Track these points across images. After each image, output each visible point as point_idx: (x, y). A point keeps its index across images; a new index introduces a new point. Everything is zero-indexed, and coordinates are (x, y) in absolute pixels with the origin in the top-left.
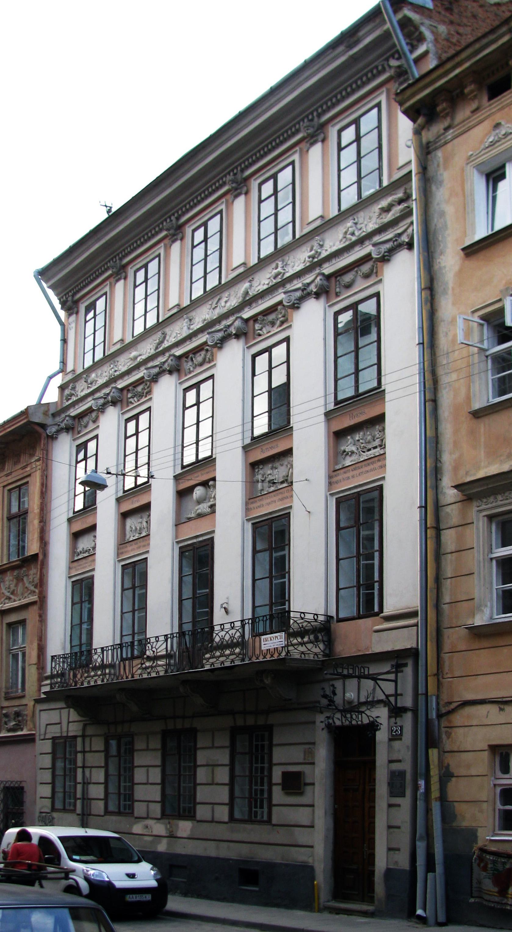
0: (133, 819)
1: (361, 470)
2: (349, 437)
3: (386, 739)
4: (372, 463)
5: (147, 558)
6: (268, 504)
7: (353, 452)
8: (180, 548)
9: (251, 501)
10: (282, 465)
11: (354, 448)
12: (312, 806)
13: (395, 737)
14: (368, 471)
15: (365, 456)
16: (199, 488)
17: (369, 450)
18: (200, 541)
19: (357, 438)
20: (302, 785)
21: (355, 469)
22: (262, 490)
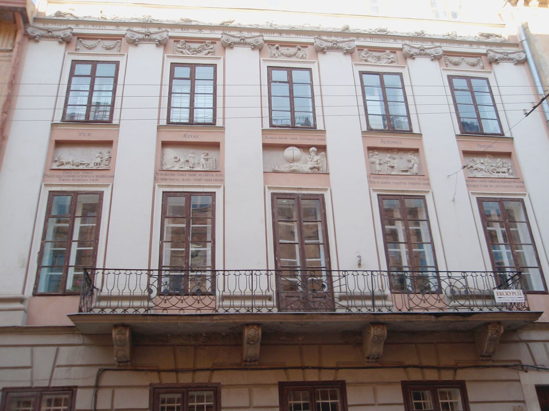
1: (498, 184)
5: (215, 193)
6: (398, 183)
7: (481, 170)
8: (273, 194)
9: (373, 176)
11: (483, 167)
14: (505, 186)
15: (496, 175)
16: (295, 148)
17: (499, 172)
18: (304, 194)
19: (482, 162)
21: (492, 181)
22: (380, 171)
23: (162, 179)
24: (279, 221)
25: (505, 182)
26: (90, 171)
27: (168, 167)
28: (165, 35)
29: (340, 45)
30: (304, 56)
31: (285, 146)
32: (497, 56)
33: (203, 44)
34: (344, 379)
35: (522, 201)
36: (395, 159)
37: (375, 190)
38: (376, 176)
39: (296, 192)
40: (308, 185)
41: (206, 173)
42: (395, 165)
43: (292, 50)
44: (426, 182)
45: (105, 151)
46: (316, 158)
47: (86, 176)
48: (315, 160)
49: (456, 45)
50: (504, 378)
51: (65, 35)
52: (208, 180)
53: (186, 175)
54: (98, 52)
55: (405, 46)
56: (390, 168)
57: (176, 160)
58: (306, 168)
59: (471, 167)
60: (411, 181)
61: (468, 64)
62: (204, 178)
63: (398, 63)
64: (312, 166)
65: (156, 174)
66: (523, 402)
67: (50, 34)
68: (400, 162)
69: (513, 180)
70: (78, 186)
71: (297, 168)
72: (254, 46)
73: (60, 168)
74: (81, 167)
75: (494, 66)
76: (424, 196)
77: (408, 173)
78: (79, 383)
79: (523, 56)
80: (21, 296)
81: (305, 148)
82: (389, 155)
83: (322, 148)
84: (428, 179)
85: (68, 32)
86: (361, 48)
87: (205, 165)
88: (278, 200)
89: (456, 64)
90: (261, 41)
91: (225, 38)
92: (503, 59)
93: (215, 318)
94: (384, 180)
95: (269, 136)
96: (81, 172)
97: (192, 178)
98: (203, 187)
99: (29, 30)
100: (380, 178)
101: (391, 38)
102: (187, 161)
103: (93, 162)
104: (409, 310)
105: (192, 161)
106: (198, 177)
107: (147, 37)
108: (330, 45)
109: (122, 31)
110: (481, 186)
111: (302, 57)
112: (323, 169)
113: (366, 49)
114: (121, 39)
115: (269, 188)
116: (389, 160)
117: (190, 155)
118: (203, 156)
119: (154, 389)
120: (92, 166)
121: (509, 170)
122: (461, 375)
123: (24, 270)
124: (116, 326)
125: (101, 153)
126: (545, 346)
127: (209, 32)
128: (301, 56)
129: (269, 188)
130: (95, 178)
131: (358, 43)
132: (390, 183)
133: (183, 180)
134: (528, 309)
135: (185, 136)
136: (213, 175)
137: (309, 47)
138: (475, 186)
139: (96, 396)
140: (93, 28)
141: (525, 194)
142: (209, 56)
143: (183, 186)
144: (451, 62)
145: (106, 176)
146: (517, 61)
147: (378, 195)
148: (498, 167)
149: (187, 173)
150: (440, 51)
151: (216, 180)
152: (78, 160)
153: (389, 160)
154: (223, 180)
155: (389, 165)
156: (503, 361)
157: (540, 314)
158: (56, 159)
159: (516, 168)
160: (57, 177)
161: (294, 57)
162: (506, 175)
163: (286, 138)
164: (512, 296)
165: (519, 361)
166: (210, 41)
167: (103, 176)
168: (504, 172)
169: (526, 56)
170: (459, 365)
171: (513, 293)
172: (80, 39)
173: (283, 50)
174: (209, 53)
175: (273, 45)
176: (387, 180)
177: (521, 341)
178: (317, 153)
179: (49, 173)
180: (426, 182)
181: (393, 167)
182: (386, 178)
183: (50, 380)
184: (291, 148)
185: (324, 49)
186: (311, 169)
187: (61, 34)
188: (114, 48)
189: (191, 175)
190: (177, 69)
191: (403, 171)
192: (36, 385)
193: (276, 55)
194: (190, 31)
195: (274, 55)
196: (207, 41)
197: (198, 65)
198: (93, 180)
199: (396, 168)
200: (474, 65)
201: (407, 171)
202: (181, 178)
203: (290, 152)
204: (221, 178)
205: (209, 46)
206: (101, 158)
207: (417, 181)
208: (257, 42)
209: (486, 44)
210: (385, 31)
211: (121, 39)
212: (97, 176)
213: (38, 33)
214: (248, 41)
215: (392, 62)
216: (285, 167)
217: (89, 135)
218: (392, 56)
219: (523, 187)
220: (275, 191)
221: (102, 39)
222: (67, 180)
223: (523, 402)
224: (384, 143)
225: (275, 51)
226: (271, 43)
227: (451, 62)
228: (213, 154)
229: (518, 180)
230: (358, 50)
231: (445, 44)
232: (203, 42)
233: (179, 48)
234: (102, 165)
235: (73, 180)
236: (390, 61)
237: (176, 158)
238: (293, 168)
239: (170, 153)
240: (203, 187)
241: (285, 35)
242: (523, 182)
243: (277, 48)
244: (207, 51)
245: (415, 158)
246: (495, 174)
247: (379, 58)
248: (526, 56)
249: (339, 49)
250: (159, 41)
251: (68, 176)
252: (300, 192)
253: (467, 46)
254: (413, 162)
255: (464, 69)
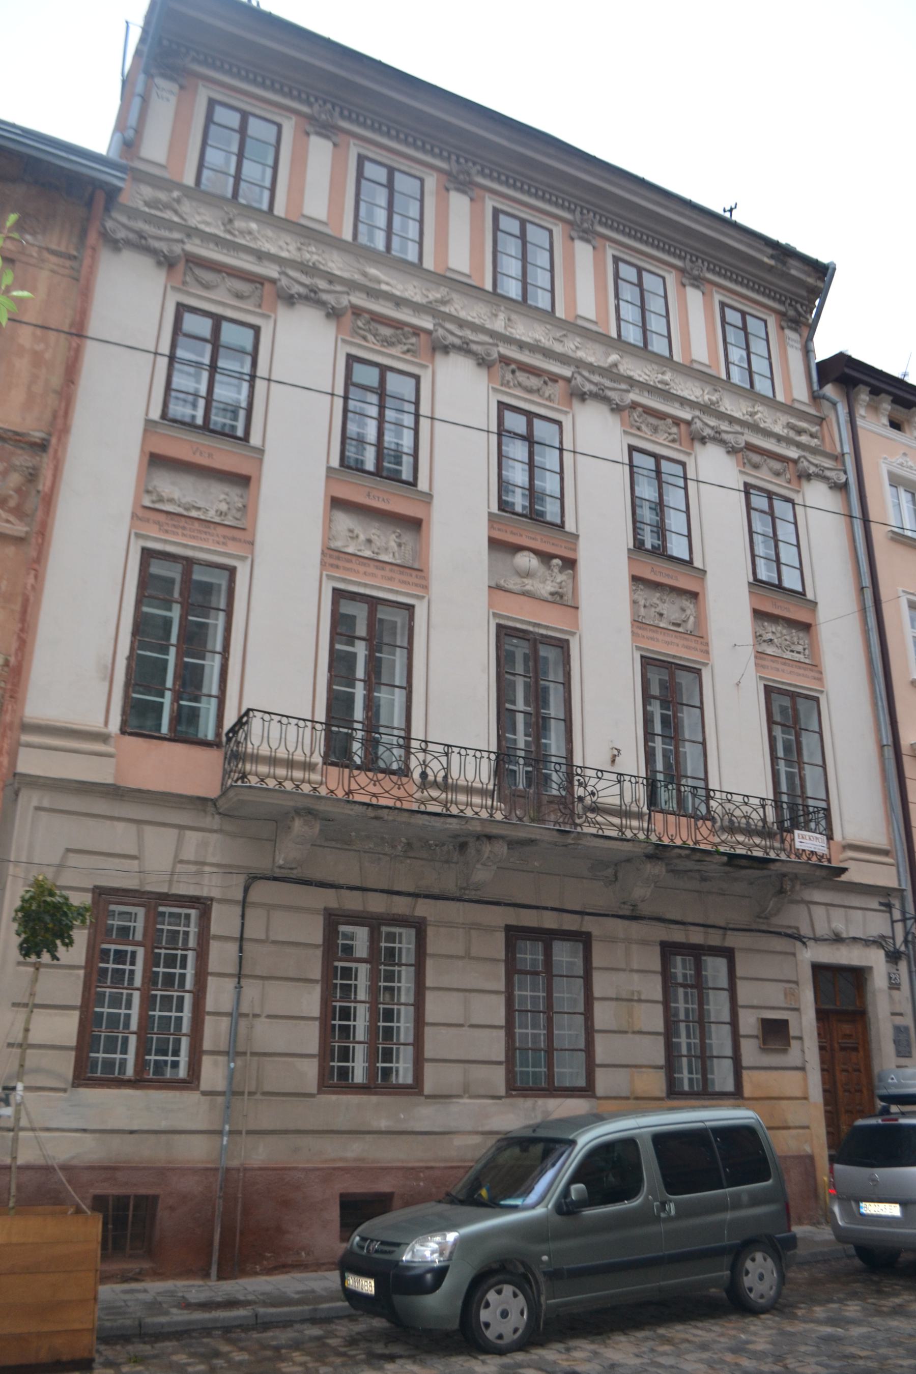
0: (423, 1098)
2: (766, 624)
3: (886, 988)
4: (805, 669)
5: (413, 606)
6: (668, 643)
10: (673, 603)
12: (802, 1069)
13: (894, 986)
15: (788, 655)
16: (532, 555)
18: (542, 635)
20: (761, 1036)
21: (784, 664)
22: (644, 617)
23: (332, 565)
24: (507, 672)
25: (800, 668)
26: (212, 526)
27: (338, 544)
28: (345, 301)
29: (609, 393)
30: (552, 396)
31: (519, 549)
32: (812, 470)
33: (399, 332)
34: (590, 930)
35: (817, 700)
36: (664, 603)
37: (638, 648)
38: (641, 625)
39: (531, 629)
40: (548, 620)
41: (402, 569)
42: (665, 612)
43: (534, 382)
44: (704, 648)
45: (234, 494)
46: (560, 578)
47: (205, 533)
48: (559, 580)
49: (760, 436)
50: (779, 949)
51: (171, 251)
52: (404, 582)
53: (369, 565)
54: (219, 298)
55: (696, 420)
56: (657, 616)
57: (351, 535)
58: (545, 588)
59: (760, 636)
60: (685, 643)
61: (771, 470)
62: (397, 576)
63: (681, 445)
64: (553, 590)
65: (323, 553)
66: (796, 983)
67: (143, 242)
68: (671, 608)
69: (810, 667)
70: (193, 548)
71: (532, 588)
72: (483, 359)
73: (158, 506)
74: (194, 514)
75: (804, 483)
76: (700, 670)
77: (680, 629)
78: (215, 893)
79: (843, 479)
80: (104, 730)
81: (545, 557)
82: (658, 595)
83: (570, 564)
84: (707, 644)
85: (177, 249)
86: (634, 405)
87: (397, 555)
88: (507, 638)
89: (756, 467)
90: (495, 356)
91: (441, 332)
92: (817, 476)
93: (450, 820)
94: (650, 634)
95: (496, 526)
96: (196, 525)
97: (380, 573)
98: (397, 592)
99: (109, 224)
100: (646, 629)
101: (677, 401)
102: (369, 541)
103: (215, 508)
104: (695, 844)
105: (378, 542)
106: (389, 574)
107: (312, 295)
108: (594, 389)
109: (271, 271)
110: (772, 668)
111: (549, 398)
112: (568, 598)
113: (640, 409)
114: (262, 284)
115: (495, 615)
116: (658, 602)
117: (374, 531)
118: (393, 536)
119: (330, 915)
120: (211, 515)
121: (804, 649)
122: (732, 940)
123: (107, 684)
124: (298, 812)
125: (227, 494)
126: (827, 911)
127: (410, 312)
128: (547, 395)
129: (495, 615)
130: (222, 540)
131: (634, 396)
132: (658, 640)
133: (365, 573)
134: (829, 861)
135: (369, 495)
136: (411, 575)
137: (561, 383)
138: (763, 666)
139: (243, 916)
140: (216, 248)
141: (822, 692)
142: (408, 357)
143: (365, 585)
144: (749, 461)
145: (240, 540)
146: (835, 483)
147: (642, 657)
148: (793, 643)
149: (372, 563)
150: (741, 441)
151: (416, 585)
152: (188, 499)
153: (658, 602)
154: (426, 588)
155: (657, 610)
156: (782, 926)
157: (844, 870)
158: (150, 488)
159: (813, 649)
160: (155, 522)
161: (536, 395)
162: (801, 657)
163: (521, 535)
164: (807, 841)
165: (797, 928)
166: (410, 330)
167: (234, 539)
168: (799, 653)
169: (847, 479)
170: (731, 926)
171: (817, 838)
172: (191, 265)
173: (522, 377)
174: (408, 351)
175: (508, 364)
176: (655, 635)
177: (803, 901)
178: (562, 569)
179: (140, 512)
180: (704, 648)
181: (661, 615)
182: (654, 631)
183: (171, 882)
184: (526, 553)
185: (585, 393)
186: (552, 594)
187: (163, 246)
188: (248, 297)
189: (377, 567)
190: (357, 367)
191: (674, 624)
192: (148, 888)
193: (511, 384)
194: (381, 301)
195: (508, 382)
196: (406, 329)
197: (392, 369)
198: (218, 543)
199: (665, 616)
200: (778, 474)
201: (679, 625)
202: (362, 569)
203: (526, 560)
204: (423, 582)
205: (407, 338)
206: (228, 503)
207: (693, 645)
208: (489, 355)
209: (799, 445)
210: (667, 384)
211: (262, 284)
212: (224, 537)
213: (121, 234)
214: (474, 347)
215: (674, 441)
216: (513, 583)
217: (210, 455)
218: (674, 430)
219: (820, 680)
220: (502, 622)
221: (228, 274)
222: (174, 533)
223: (796, 983)
224: (655, 574)
225: (509, 376)
226: (505, 361)
227: (749, 461)
228: (408, 538)
229: (815, 668)
230: (631, 407)
231: (746, 431)
232: (397, 328)
233: (360, 328)
234: (230, 517)
235: (184, 535)
236: (671, 437)
237: (351, 531)
238: (528, 588)
239: (344, 521)
240: (397, 592)
241: (527, 352)
242: (821, 673)
243: (513, 372)
244: (405, 348)
245: (692, 606)
246: (788, 652)
247: (655, 430)
248: (847, 479)
249: (606, 400)
250: (333, 308)
251: (175, 526)
252: (537, 630)
253: (773, 441)
254: (688, 612)
255: (764, 477)
